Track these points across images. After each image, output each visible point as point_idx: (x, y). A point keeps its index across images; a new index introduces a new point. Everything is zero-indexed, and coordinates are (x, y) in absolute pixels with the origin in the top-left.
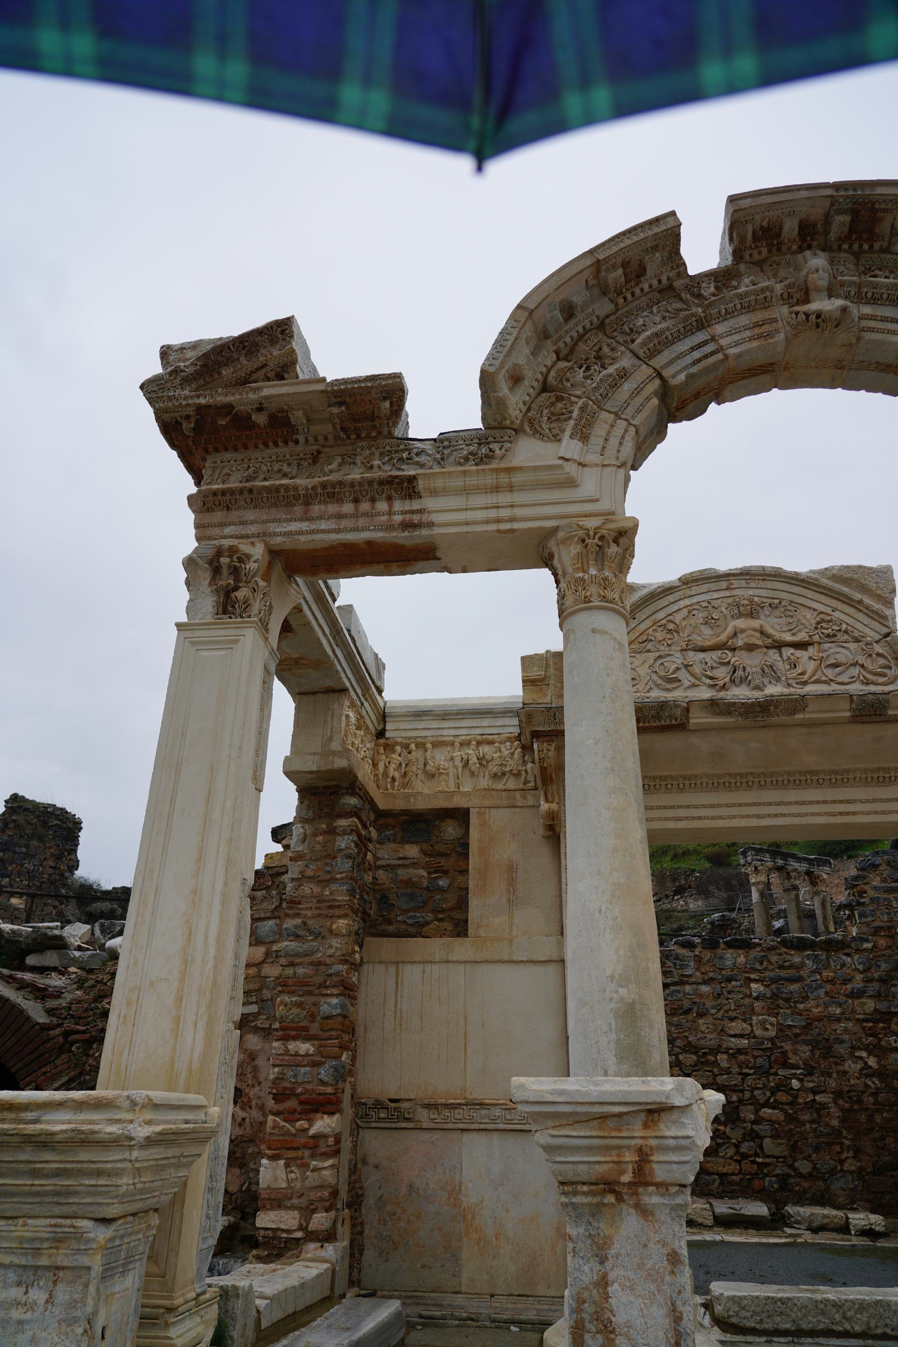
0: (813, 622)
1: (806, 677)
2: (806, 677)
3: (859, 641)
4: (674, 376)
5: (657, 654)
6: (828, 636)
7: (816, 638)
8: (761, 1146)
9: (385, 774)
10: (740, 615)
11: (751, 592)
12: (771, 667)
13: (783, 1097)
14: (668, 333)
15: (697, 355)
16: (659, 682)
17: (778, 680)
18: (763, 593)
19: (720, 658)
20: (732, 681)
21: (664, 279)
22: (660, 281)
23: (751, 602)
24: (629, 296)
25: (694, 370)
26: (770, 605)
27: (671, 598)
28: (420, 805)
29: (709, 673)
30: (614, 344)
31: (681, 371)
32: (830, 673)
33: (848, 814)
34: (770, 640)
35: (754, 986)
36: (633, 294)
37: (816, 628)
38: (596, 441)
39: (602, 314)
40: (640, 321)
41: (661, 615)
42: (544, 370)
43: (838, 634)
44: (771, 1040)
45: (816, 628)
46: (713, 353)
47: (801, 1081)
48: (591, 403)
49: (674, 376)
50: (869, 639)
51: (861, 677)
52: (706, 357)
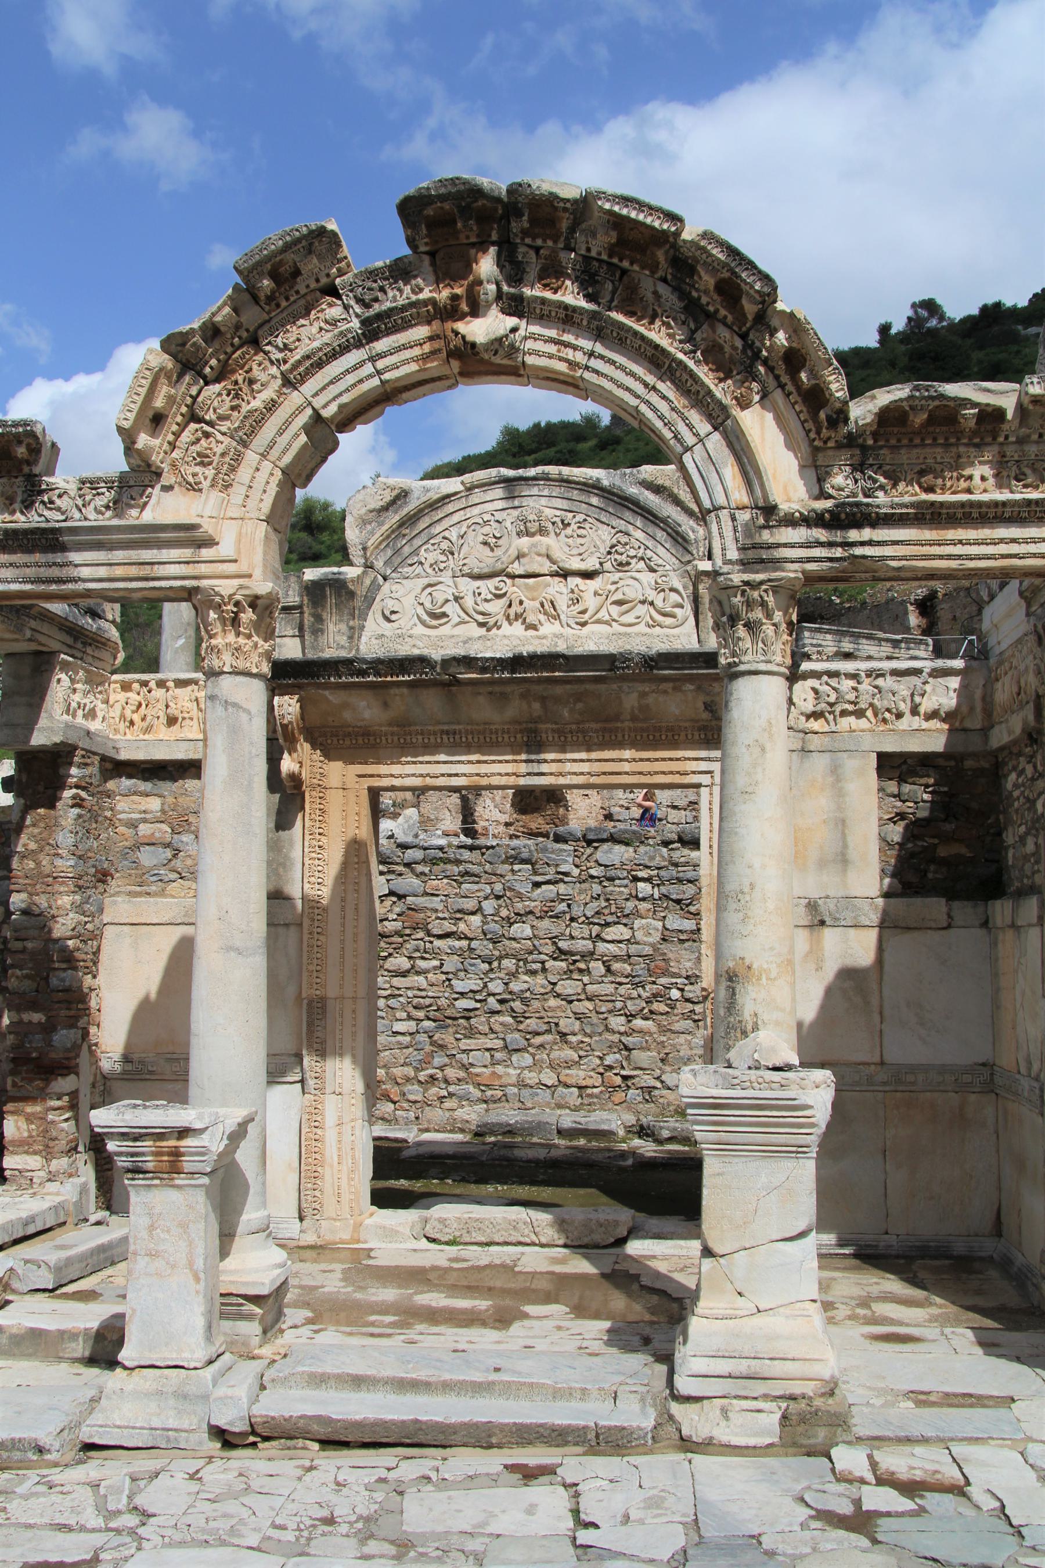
2: (586, 616)
3: (655, 571)
4: (325, 406)
5: (426, 581)
6: (621, 564)
8: (628, 1058)
9: (123, 717)
11: (544, 501)
12: (552, 602)
13: (655, 1006)
14: (321, 354)
15: (351, 379)
16: (425, 617)
17: (557, 617)
19: (497, 588)
22: (318, 281)
25: (345, 399)
26: (562, 521)
27: (450, 508)
29: (480, 608)
30: (267, 363)
31: (334, 399)
32: (615, 610)
34: (555, 568)
35: (641, 885)
36: (287, 299)
37: (609, 553)
38: (238, 492)
40: (291, 337)
41: (438, 529)
42: (189, 400)
44: (652, 945)
45: (609, 553)
46: (370, 376)
47: (682, 990)
48: (235, 444)
49: (325, 406)
50: (668, 567)
52: (361, 381)
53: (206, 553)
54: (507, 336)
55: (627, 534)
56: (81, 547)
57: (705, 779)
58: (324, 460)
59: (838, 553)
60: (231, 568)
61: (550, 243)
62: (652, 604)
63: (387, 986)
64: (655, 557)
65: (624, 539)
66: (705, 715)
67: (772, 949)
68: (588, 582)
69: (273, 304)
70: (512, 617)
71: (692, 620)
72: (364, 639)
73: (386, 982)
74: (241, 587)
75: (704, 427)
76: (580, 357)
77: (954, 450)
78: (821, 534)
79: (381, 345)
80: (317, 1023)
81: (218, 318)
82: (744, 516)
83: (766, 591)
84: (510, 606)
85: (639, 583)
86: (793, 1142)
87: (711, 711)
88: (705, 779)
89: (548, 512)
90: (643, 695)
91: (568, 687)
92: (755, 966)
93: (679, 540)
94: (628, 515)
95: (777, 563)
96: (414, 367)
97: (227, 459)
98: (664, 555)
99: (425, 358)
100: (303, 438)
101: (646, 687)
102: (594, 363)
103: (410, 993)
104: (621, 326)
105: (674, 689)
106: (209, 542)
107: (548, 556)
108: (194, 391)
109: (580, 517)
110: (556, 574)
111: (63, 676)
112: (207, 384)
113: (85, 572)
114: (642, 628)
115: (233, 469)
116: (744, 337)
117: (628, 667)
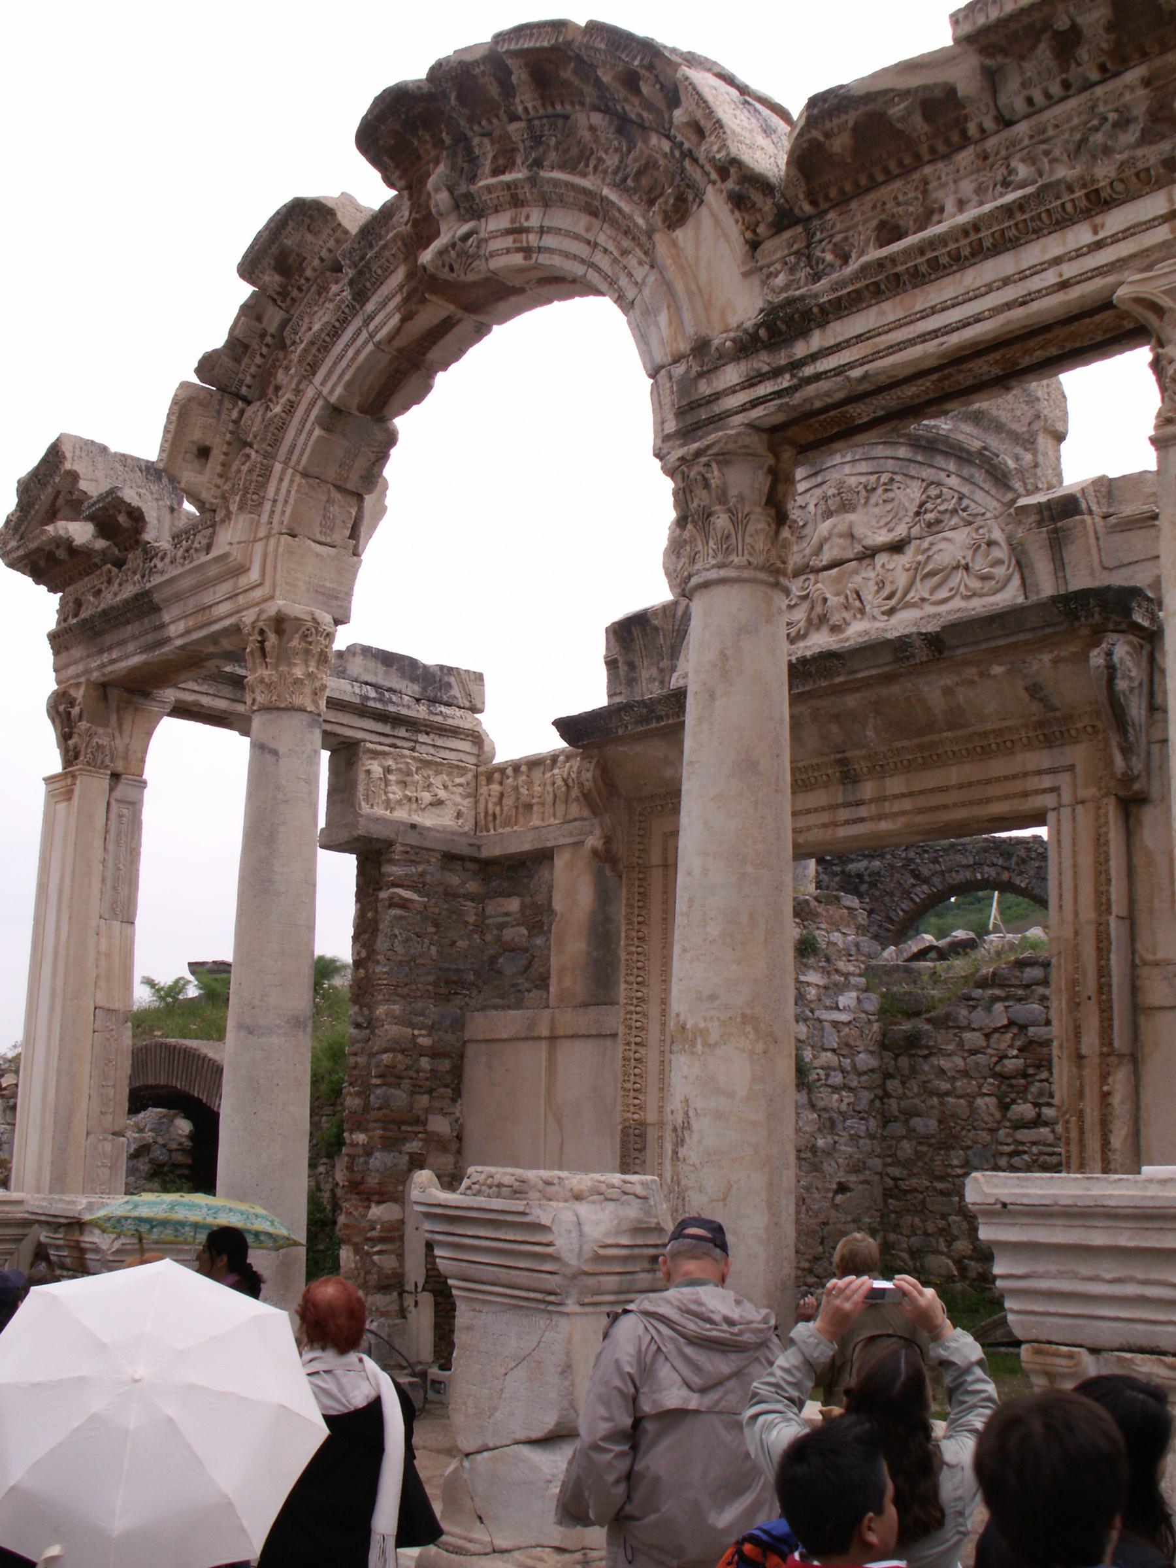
0: (917, 502)
1: (893, 602)
2: (893, 602)
3: (970, 523)
7: (915, 531)
9: (486, 813)
10: (828, 514)
11: (847, 469)
15: (350, 353)
18: (863, 467)
20: (809, 621)
21: (324, 253)
22: (322, 260)
23: (840, 484)
24: (295, 293)
25: (347, 377)
28: (513, 848)
33: (937, 808)
36: (300, 289)
39: (272, 329)
42: (231, 426)
43: (947, 516)
45: (918, 514)
51: (962, 588)
53: (243, 581)
54: (454, 245)
55: (939, 484)
56: (169, 601)
57: (1049, 800)
58: (382, 457)
59: (785, 381)
61: (495, 121)
62: (967, 568)
63: (1010, 1140)
64: (973, 505)
65: (933, 492)
66: (1035, 707)
67: (713, 997)
68: (896, 557)
69: (288, 300)
70: (815, 621)
71: (1016, 581)
72: (673, 680)
73: (1008, 1135)
74: (261, 612)
75: (639, 273)
76: (533, 239)
77: (916, 176)
78: (762, 362)
79: (370, 307)
80: (634, 1154)
81: (237, 332)
82: (679, 370)
83: (707, 465)
84: (812, 608)
85: (953, 545)
86: (536, 1285)
87: (1041, 700)
88: (1049, 800)
89: (853, 481)
90: (948, 692)
91: (859, 695)
92: (688, 1026)
93: (1000, 478)
94: (940, 461)
95: (720, 418)
97: (254, 477)
98: (986, 501)
99: (407, 300)
100: (318, 432)
101: (948, 680)
102: (549, 241)
103: (1035, 1150)
104: (556, 183)
105: (981, 675)
106: (241, 570)
107: (852, 536)
108: (235, 415)
109: (884, 478)
110: (860, 558)
111: (376, 768)
112: (249, 403)
114: (957, 603)
115: (263, 485)
116: (668, 137)
117: (912, 656)
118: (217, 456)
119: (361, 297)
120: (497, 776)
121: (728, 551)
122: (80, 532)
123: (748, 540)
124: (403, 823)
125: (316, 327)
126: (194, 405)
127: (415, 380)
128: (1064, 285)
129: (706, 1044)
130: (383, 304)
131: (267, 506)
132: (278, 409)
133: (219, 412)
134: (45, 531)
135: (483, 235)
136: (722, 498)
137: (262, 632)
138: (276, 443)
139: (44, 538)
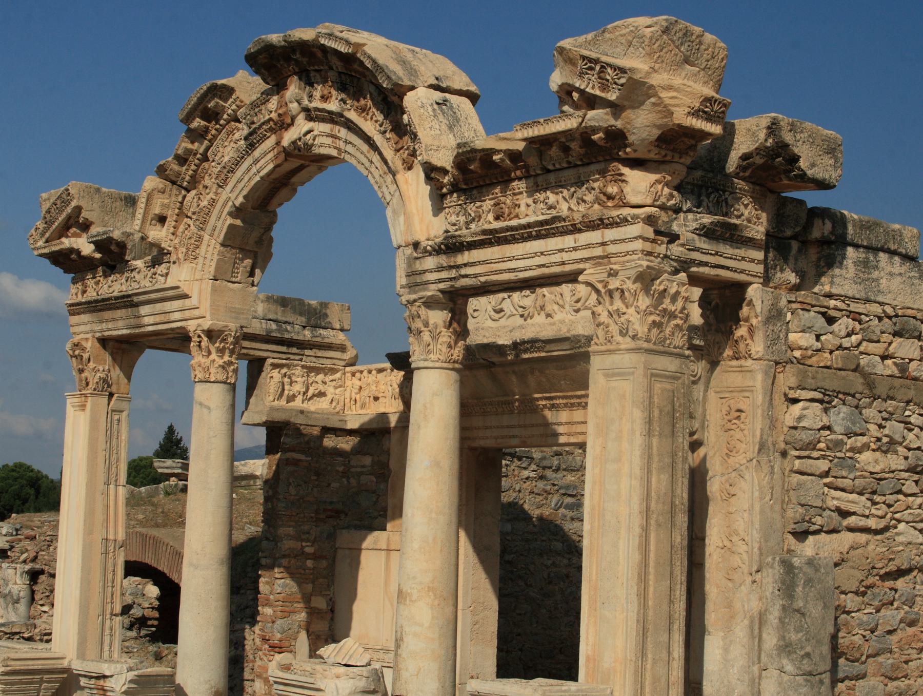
15: (246, 179)
25: (245, 192)
54: (300, 139)
60: (196, 313)
67: (414, 578)
74: (199, 325)
79: (257, 153)
96: (271, 166)
108: (180, 199)
111: (275, 373)
112: (188, 191)
113: (146, 320)
118: (170, 222)
119: (252, 146)
120: (358, 375)
121: (429, 352)
122: (86, 248)
123: (439, 346)
124: (297, 411)
125: (226, 159)
126: (155, 192)
127: (284, 192)
128: (563, 263)
129: (411, 601)
130: (265, 154)
131: (201, 260)
132: (205, 203)
133: (170, 195)
134: (63, 243)
135: (316, 133)
136: (426, 325)
137: (199, 336)
138: (205, 222)
139: (62, 247)
